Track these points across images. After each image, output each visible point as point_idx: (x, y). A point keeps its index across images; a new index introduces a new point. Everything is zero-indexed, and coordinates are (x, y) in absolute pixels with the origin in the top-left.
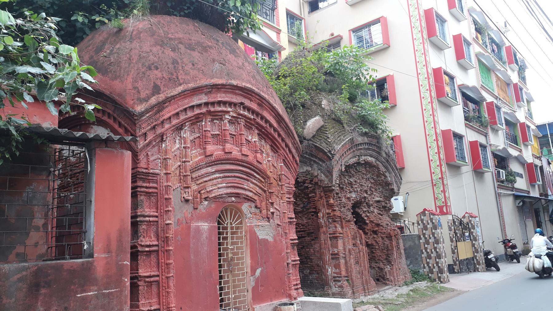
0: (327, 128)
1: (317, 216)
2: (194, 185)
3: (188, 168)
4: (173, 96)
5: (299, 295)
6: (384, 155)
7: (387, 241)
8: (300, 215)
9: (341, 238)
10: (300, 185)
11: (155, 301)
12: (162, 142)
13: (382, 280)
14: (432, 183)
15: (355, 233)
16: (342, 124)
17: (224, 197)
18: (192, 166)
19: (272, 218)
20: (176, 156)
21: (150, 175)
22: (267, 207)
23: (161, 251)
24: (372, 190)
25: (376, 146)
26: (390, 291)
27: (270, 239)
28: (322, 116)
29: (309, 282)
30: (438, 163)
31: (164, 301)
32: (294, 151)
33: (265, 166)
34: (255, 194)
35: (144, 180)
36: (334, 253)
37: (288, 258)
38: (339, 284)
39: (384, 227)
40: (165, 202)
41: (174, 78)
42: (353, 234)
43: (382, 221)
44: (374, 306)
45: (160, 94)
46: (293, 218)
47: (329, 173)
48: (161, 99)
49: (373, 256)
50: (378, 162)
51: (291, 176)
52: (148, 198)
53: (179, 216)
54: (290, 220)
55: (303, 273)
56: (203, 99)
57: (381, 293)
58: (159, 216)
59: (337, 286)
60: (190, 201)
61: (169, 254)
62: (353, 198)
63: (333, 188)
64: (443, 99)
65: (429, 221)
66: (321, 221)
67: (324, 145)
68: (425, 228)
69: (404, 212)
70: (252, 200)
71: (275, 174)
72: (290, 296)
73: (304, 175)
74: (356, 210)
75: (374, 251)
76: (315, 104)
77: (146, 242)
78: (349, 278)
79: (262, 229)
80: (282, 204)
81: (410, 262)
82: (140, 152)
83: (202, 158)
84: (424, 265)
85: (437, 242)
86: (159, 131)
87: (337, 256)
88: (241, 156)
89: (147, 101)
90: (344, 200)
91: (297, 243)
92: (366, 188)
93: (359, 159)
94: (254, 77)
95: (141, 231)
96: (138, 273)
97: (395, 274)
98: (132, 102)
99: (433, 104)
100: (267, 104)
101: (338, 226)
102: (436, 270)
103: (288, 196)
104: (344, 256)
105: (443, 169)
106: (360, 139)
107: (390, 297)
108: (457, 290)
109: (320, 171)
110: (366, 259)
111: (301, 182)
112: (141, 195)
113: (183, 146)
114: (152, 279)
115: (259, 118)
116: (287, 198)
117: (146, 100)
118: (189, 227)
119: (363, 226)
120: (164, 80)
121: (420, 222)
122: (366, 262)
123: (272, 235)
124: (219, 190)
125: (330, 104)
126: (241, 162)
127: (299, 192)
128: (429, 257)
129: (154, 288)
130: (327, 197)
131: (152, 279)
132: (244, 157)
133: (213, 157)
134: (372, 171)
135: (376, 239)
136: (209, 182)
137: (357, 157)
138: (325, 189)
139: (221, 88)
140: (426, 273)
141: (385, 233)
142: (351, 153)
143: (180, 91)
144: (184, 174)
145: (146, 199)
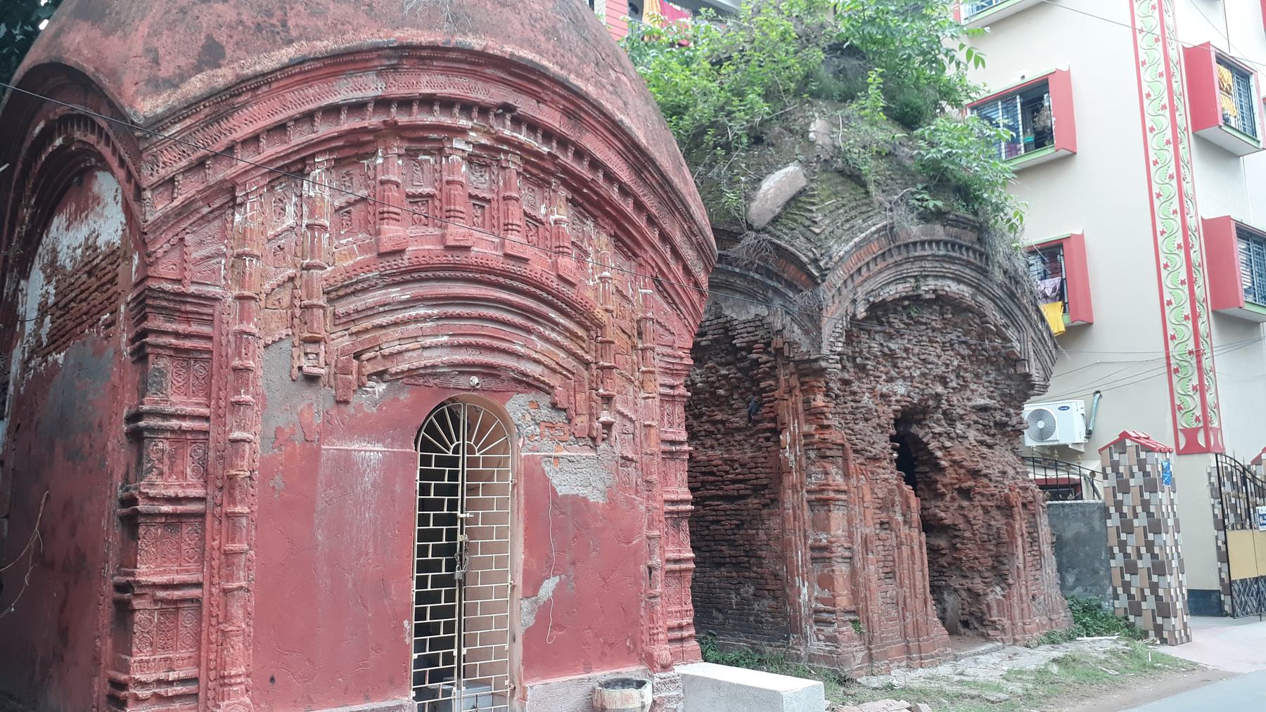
0: (814, 195)
1: (778, 442)
2: (342, 336)
3: (319, 286)
4: (264, 75)
5: (682, 657)
6: (999, 276)
7: (998, 517)
8: (738, 438)
9: (840, 503)
10: (739, 356)
11: (188, 655)
12: (233, 207)
13: (976, 625)
14: (1169, 364)
15: (891, 492)
16: (864, 185)
18: (331, 281)
19: (603, 439)
20: (282, 249)
21: (189, 300)
22: (591, 407)
23: (214, 515)
24: (964, 378)
25: (975, 251)
26: (994, 658)
28: (806, 164)
29: (752, 619)
30: (1188, 311)
31: (212, 656)
32: (689, 254)
33: (589, 294)
34: (554, 371)
35: (170, 314)
36: (818, 544)
37: (651, 552)
38: (829, 630)
39: (994, 478)
40: (231, 377)
41: (273, 25)
42: (880, 496)
43: (988, 463)
44: (908, 705)
45: (219, 66)
46: (681, 443)
47: (812, 320)
48: (220, 83)
49: (955, 558)
50: (980, 299)
51: (681, 325)
52: (185, 364)
53: (281, 419)
54: (668, 448)
55: (740, 594)
56: (372, 87)
57: (963, 661)
58: (212, 417)
59: (821, 637)
60: (324, 380)
61: (234, 524)
62: (898, 398)
63: (823, 364)
64: (1210, 133)
65: (1135, 469)
66: (787, 454)
67: (801, 242)
68: (1124, 487)
69: (1085, 444)
70: (542, 385)
71: (624, 318)
72: (649, 660)
73: (750, 329)
74: (912, 431)
75: (959, 545)
76: (791, 131)
77: (167, 487)
78: (858, 616)
79: (567, 467)
80: (643, 402)
81: (1077, 579)
82: (154, 232)
83: (369, 260)
84: (1115, 589)
85: (1156, 526)
86: (220, 173)
87: (826, 554)
88: (501, 259)
89: (177, 87)
90: (866, 399)
91: (689, 511)
92: (941, 370)
93: (918, 287)
94: (551, 33)
95: (153, 456)
96: (133, 574)
97: (1017, 612)
98: (134, 89)
99: (1181, 147)
100: (595, 114)
101: (833, 470)
102: (1148, 605)
103: (669, 381)
104: (847, 554)
105: (1202, 328)
106: (915, 230)
107: (982, 676)
108: (1204, 669)
109: (789, 318)
110: (917, 566)
111: (742, 349)
112: (158, 356)
113: (305, 221)
114: (177, 594)
115: (570, 155)
116: (661, 385)
117: (175, 82)
118: (317, 453)
119: (931, 474)
120: (240, 28)
121: (1109, 470)
122: (918, 575)
123: (601, 486)
124: (427, 353)
125: (835, 130)
126: (505, 277)
127: (739, 375)
128: (1131, 568)
129: (186, 619)
130: (805, 390)
131: (177, 594)
132: (513, 263)
133: (406, 257)
134: (963, 322)
135: (966, 513)
136: (391, 330)
137: (912, 280)
138: (800, 367)
139: (431, 58)
140: (1120, 614)
141: (993, 495)
142: (887, 268)
143: (287, 61)
144: (306, 302)
145: (175, 367)
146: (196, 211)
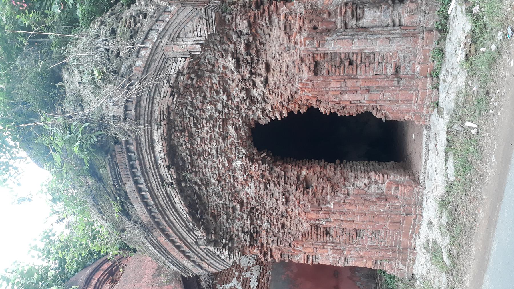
9: (314, 259)
50: (157, 115)
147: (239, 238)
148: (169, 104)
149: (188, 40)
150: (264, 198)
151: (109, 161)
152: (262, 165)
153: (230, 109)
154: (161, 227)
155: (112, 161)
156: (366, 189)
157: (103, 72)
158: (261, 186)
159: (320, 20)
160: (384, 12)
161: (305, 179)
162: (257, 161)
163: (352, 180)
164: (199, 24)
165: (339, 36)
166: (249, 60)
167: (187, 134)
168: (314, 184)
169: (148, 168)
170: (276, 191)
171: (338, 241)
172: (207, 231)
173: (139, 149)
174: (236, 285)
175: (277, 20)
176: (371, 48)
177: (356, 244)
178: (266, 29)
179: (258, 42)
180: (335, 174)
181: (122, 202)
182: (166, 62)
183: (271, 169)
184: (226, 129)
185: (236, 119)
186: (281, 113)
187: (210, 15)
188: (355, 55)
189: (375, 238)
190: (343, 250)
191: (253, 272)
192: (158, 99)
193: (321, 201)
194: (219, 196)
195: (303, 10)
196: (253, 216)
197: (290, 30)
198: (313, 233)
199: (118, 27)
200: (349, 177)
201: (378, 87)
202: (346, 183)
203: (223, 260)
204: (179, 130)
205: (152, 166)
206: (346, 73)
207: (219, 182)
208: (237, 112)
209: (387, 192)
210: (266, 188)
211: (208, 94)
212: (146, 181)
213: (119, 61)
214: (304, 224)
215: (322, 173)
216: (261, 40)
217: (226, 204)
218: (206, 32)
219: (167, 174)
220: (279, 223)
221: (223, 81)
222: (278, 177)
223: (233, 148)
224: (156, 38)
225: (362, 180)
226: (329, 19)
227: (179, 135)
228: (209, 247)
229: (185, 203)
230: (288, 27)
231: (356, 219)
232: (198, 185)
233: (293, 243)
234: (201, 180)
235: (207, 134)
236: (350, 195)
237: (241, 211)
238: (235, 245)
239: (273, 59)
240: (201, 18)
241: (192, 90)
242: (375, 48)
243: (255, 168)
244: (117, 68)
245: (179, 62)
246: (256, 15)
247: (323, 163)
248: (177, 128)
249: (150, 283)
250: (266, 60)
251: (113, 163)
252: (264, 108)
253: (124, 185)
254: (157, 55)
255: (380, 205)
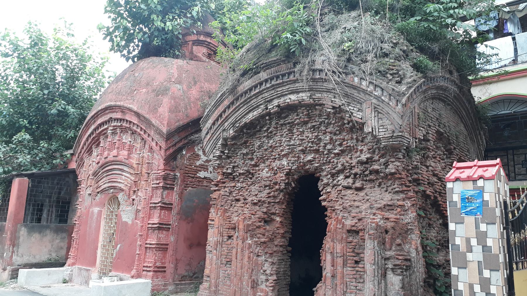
9: (212, 225)
17: (108, 190)
27: (130, 222)
50: (318, 95)
146: (81, 164)
147: (230, 163)
148: (326, 106)
149: (376, 121)
150: (259, 185)
151: (280, 59)
152: (285, 183)
153: (327, 156)
154: (235, 101)
155: (280, 61)
156: (262, 271)
157: (349, 50)
158: (268, 182)
159: (394, 237)
160: (398, 293)
161: (273, 220)
162: (288, 179)
163: (270, 260)
164: (389, 130)
165: (377, 252)
166: (366, 173)
167: (306, 119)
168: (268, 227)
169: (277, 90)
170: (263, 195)
171: (223, 246)
172: (234, 138)
173: (291, 82)
174: (202, 160)
175: (399, 198)
176: (368, 280)
177: (221, 261)
178: (391, 188)
179: (381, 180)
180: (276, 246)
181: (252, 70)
182: (359, 103)
183: (282, 191)
184: (311, 153)
185: (320, 161)
186: (324, 200)
187: (396, 140)
188: (362, 266)
189: (225, 277)
190: (216, 250)
191: (212, 173)
192: (330, 96)
193: (253, 233)
194: (260, 147)
195: (406, 221)
196: (246, 174)
197: (388, 210)
198: (230, 225)
199: (390, 59)
200: (273, 258)
201: (336, 285)
202: (268, 255)
203: (212, 152)
204: (309, 113)
205: (279, 92)
206: (349, 257)
207: (271, 147)
208: (325, 161)
209: (259, 288)
210: (266, 186)
211: (338, 137)
212: (268, 88)
213: (358, 62)
214: (237, 218)
215: (278, 235)
216: (383, 183)
217: (255, 152)
218: (382, 136)
219: (274, 105)
220: (240, 197)
221: (350, 150)
222: (274, 197)
223: (296, 159)
224: (376, 94)
225: (270, 269)
226: (394, 245)
227: (304, 113)
228: (221, 139)
229: (253, 119)
230: (391, 208)
231: (238, 261)
232: (268, 130)
233: (223, 208)
234: (271, 132)
235: (306, 137)
236: (257, 258)
237: (250, 165)
238: (224, 161)
239: (366, 194)
240: (393, 132)
241: (339, 124)
242: (368, 283)
243: (282, 177)
244: (352, 60)
245: (358, 113)
246: (402, 180)
247: (288, 235)
248: (310, 111)
249: (203, 90)
250: (366, 188)
251: (279, 62)
252: (329, 185)
253: (264, 71)
254: (363, 95)
255: (248, 282)
